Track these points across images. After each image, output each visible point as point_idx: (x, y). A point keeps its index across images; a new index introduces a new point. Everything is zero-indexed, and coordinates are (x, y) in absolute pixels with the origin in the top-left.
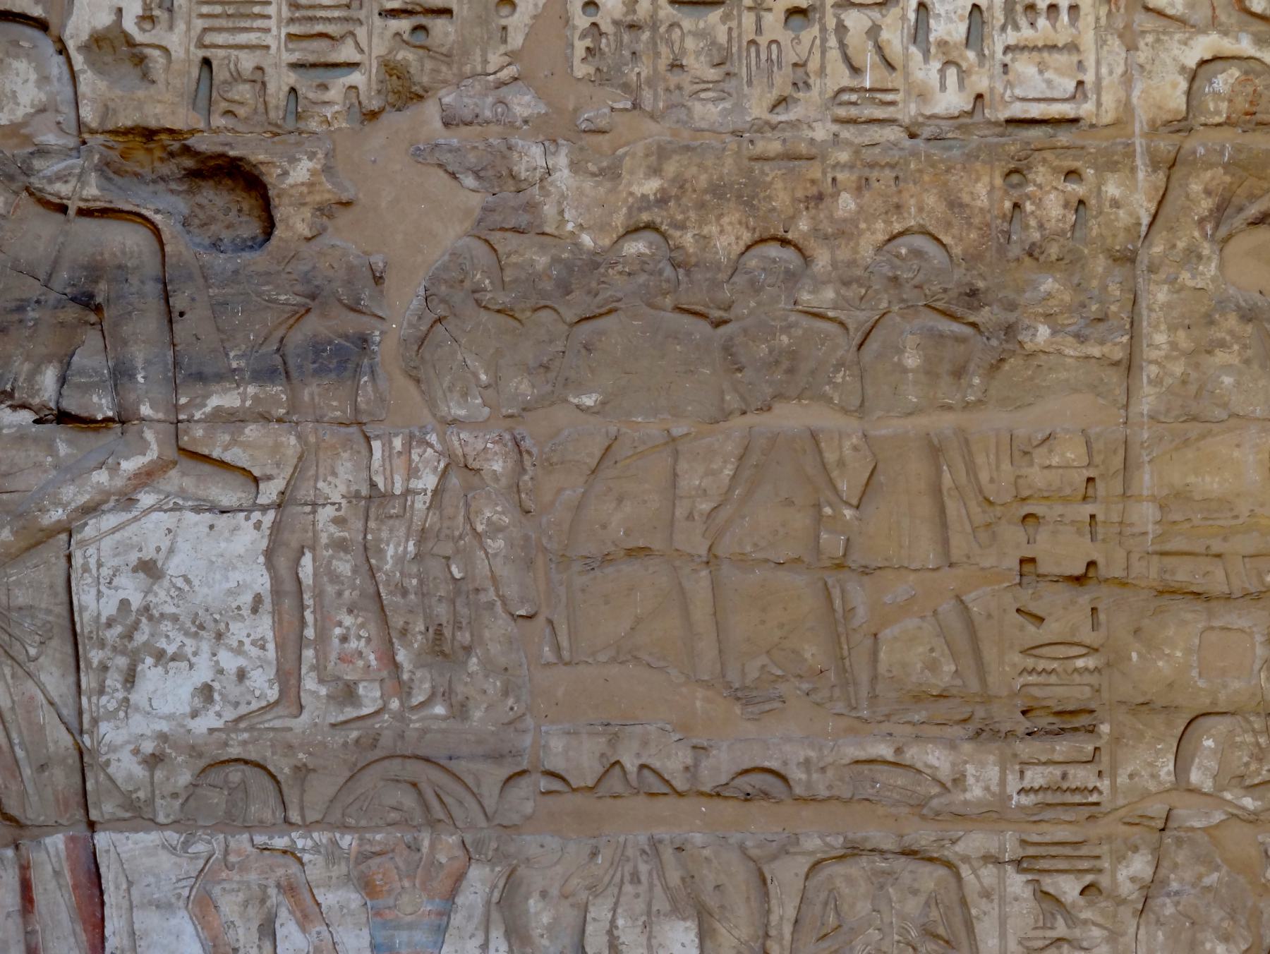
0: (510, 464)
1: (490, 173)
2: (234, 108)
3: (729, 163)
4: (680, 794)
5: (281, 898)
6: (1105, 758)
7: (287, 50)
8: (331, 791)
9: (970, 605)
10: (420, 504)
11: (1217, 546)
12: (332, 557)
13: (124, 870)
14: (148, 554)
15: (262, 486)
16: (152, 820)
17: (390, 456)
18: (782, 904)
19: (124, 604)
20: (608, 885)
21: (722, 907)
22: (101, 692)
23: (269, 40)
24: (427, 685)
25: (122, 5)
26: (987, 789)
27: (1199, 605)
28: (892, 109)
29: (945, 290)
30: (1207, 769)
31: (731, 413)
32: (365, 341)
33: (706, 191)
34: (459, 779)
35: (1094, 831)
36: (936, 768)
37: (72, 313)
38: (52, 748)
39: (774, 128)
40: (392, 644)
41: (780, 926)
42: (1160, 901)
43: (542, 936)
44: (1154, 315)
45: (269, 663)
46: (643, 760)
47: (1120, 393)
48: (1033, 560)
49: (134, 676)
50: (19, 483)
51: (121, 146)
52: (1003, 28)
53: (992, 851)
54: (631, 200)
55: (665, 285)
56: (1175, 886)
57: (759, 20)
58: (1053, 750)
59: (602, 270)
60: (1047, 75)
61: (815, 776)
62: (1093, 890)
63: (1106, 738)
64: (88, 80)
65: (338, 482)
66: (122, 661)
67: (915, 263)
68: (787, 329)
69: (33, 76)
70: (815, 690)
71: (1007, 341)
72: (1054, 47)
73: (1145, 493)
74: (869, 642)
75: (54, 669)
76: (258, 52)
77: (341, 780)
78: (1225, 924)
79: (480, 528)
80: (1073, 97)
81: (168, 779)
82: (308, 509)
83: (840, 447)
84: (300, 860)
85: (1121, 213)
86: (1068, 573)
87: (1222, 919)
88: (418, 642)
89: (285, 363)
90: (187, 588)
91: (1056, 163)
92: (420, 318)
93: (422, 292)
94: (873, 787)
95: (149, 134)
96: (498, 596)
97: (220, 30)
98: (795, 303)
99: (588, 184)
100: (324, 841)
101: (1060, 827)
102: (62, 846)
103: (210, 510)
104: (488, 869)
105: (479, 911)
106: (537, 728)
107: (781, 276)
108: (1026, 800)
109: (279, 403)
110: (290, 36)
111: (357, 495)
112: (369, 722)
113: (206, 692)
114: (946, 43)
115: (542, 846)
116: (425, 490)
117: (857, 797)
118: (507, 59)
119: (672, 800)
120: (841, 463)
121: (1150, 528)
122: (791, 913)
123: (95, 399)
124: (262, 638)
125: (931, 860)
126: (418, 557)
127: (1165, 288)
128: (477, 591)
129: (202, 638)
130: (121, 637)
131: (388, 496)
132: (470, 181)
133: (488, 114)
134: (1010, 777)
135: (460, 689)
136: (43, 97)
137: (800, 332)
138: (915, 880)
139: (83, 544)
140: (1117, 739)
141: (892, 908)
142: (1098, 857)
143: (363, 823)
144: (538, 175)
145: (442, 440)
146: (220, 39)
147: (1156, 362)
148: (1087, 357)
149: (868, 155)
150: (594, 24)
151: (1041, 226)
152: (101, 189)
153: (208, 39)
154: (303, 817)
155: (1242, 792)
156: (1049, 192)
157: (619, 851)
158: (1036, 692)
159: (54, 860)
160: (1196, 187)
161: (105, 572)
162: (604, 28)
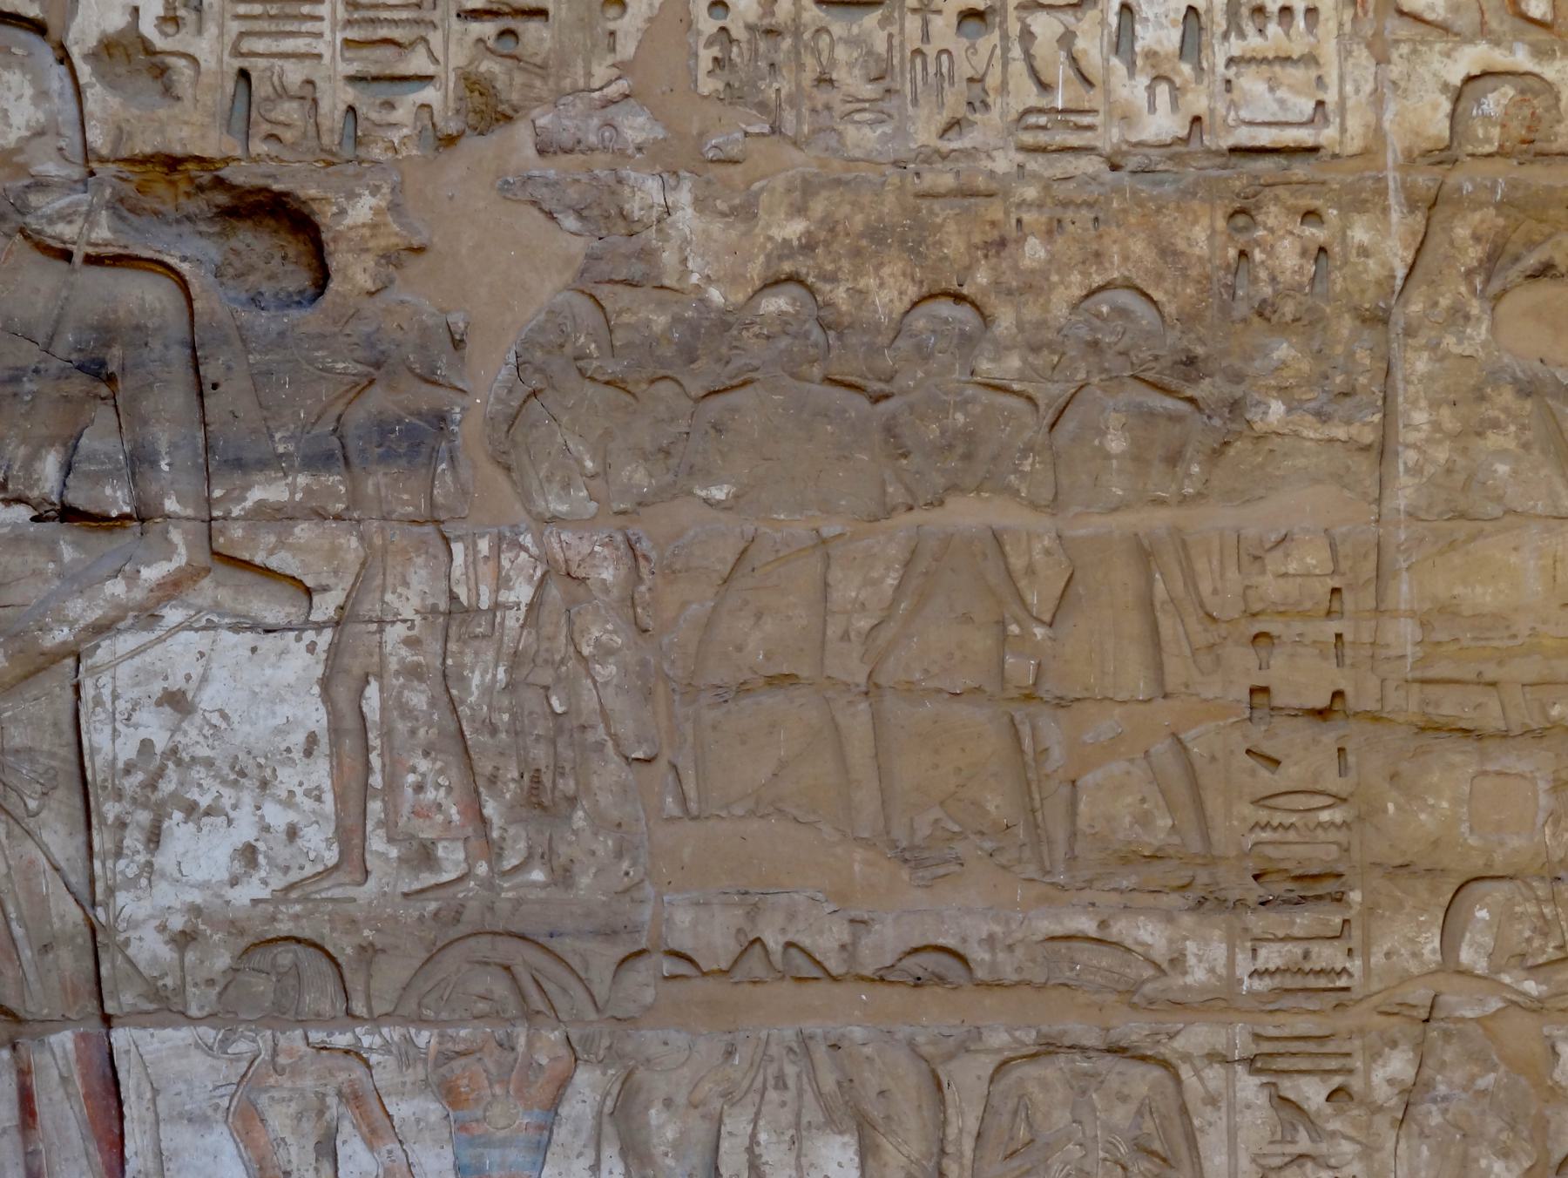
0: (623, 571)
1: (596, 212)
2: (278, 131)
4: (835, 979)
5: (342, 1109)
6: (1356, 932)
7: (344, 59)
8: (406, 975)
9: (1189, 745)
10: (512, 620)
11: (1491, 673)
12: (403, 687)
13: (148, 1075)
14: (176, 683)
15: (316, 599)
16: (183, 1013)
17: (475, 563)
18: (961, 1113)
19: (146, 745)
20: (746, 1093)
21: (888, 1118)
22: (119, 854)
23: (321, 47)
24: (522, 845)
26: (1212, 970)
27: (1470, 745)
28: (1089, 134)
29: (1156, 358)
30: (1481, 945)
31: (894, 509)
32: (443, 419)
33: (862, 235)
34: (560, 959)
35: (1343, 1022)
36: (1150, 946)
37: (78, 385)
38: (57, 925)
39: (944, 157)
41: (959, 1142)
42: (1424, 1107)
43: (666, 1154)
44: (1411, 389)
45: (327, 818)
46: (789, 937)
47: (1370, 484)
48: (1265, 690)
49: (159, 835)
50: (14, 596)
51: (136, 178)
52: (1226, 36)
53: (1219, 1047)
54: (769, 246)
55: (812, 351)
56: (1442, 1089)
57: (926, 23)
58: (1293, 923)
59: (734, 332)
60: (1280, 93)
62: (1341, 1094)
64: (96, 96)
65: (410, 594)
66: (144, 817)
67: (1119, 324)
68: (963, 404)
69: (28, 92)
70: (1000, 849)
71: (1232, 421)
72: (1288, 59)
73: (1403, 607)
74: (1065, 790)
75: (59, 826)
76: (308, 62)
77: (417, 964)
78: (1503, 1136)
79: (586, 651)
80: (1311, 121)
81: (202, 962)
82: (374, 627)
83: (1029, 550)
84: (366, 1062)
85: (1371, 263)
87: (1500, 1131)
89: (343, 447)
90: (224, 725)
91: (1291, 201)
92: (510, 391)
93: (512, 359)
94: (1072, 969)
95: (172, 163)
96: (609, 734)
98: (972, 373)
99: (717, 227)
100: (396, 1038)
101: (1300, 1018)
102: (70, 1046)
103: (252, 629)
104: (598, 1072)
105: (588, 1124)
106: (659, 895)
107: (955, 341)
108: (1259, 985)
109: (338, 499)
110: (347, 43)
111: (434, 610)
112: (451, 891)
113: (248, 854)
114: (1155, 54)
115: (666, 1043)
116: (518, 604)
117: (1053, 982)
118: (616, 72)
119: (825, 987)
120: (1031, 570)
121: (1409, 650)
122: (972, 1125)
123: (108, 491)
124: (318, 788)
125: (1144, 1058)
126: (510, 687)
127: (1425, 355)
128: (583, 728)
130: (143, 785)
131: (472, 611)
132: (570, 222)
133: (593, 139)
134: (1240, 957)
135: (563, 850)
136: (41, 117)
137: (978, 409)
138: (1124, 1083)
139: (95, 671)
140: (1370, 910)
141: (1097, 1118)
142: (1348, 1055)
143: (444, 1015)
144: (655, 214)
145: (539, 542)
146: (260, 45)
147: (1414, 446)
148: (1331, 440)
149: (1061, 191)
150: (723, 29)
151: (1273, 280)
152: (114, 231)
153: (246, 45)
155: (1523, 974)
156: (1283, 238)
158: (1270, 851)
159: (60, 1063)
160: (1462, 232)
161: (122, 705)
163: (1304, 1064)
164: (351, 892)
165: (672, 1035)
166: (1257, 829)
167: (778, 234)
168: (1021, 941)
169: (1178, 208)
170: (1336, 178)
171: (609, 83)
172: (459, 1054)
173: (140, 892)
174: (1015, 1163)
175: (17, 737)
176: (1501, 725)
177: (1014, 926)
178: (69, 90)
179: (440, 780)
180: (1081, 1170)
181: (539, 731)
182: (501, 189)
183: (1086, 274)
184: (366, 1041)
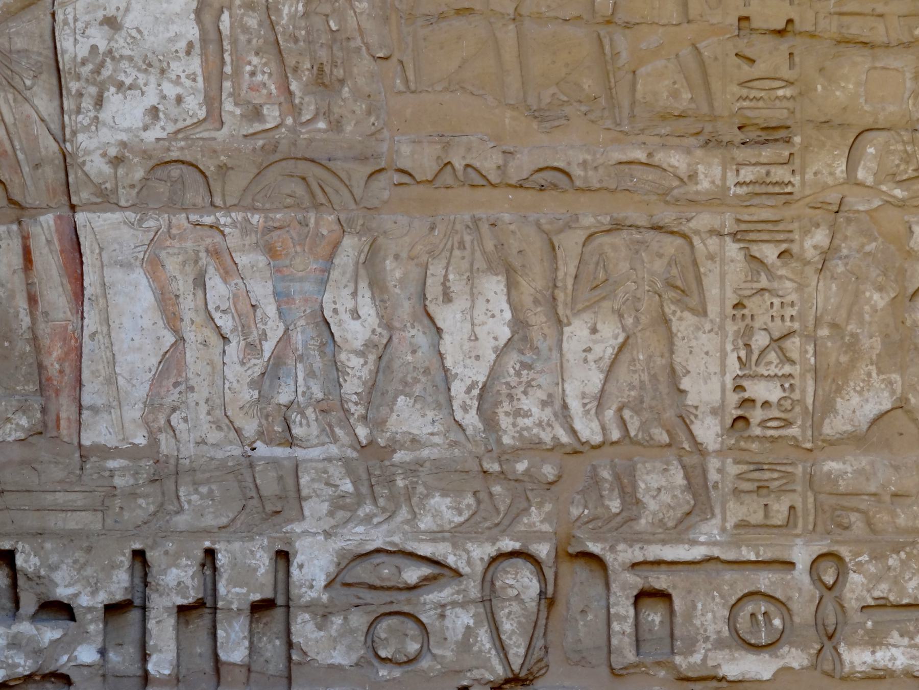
4: (494, 186)
5: (209, 259)
6: (797, 161)
8: (244, 183)
9: (702, 51)
12: (243, 15)
13: (97, 239)
14: (111, 12)
18: (566, 264)
19: (94, 48)
21: (523, 266)
22: (78, 111)
24: (312, 107)
26: (713, 182)
27: (866, 51)
34: (335, 174)
35: (788, 213)
36: (677, 168)
38: (44, 152)
40: (287, 77)
41: (564, 280)
42: (834, 262)
43: (395, 286)
46: (468, 161)
48: (747, 18)
53: (716, 226)
56: (845, 252)
58: (760, 155)
61: (590, 173)
62: (786, 254)
63: (798, 147)
66: (93, 90)
74: (630, 76)
75: (44, 96)
77: (252, 176)
78: (880, 279)
81: (127, 174)
84: (222, 232)
87: (878, 275)
88: (306, 76)
90: (139, 37)
94: (632, 181)
96: (363, 42)
100: (240, 219)
101: (764, 210)
102: (52, 223)
104: (356, 239)
105: (350, 269)
112: (271, 134)
113: (154, 112)
115: (395, 223)
119: (488, 189)
122: (572, 270)
124: (194, 74)
125: (672, 233)
126: (306, 15)
129: (150, 73)
130: (92, 72)
134: (729, 174)
135: (336, 110)
138: (661, 247)
140: (806, 147)
142: (791, 231)
143: (267, 206)
154: (225, 203)
155: (894, 185)
157: (450, 227)
158: (748, 113)
159: (46, 232)
161: (80, 25)
166: (741, 100)
168: (602, 164)
173: (91, 134)
174: (598, 292)
175: (19, 43)
176: (885, 40)
177: (598, 156)
179: (265, 69)
181: (323, 41)
184: (222, 220)
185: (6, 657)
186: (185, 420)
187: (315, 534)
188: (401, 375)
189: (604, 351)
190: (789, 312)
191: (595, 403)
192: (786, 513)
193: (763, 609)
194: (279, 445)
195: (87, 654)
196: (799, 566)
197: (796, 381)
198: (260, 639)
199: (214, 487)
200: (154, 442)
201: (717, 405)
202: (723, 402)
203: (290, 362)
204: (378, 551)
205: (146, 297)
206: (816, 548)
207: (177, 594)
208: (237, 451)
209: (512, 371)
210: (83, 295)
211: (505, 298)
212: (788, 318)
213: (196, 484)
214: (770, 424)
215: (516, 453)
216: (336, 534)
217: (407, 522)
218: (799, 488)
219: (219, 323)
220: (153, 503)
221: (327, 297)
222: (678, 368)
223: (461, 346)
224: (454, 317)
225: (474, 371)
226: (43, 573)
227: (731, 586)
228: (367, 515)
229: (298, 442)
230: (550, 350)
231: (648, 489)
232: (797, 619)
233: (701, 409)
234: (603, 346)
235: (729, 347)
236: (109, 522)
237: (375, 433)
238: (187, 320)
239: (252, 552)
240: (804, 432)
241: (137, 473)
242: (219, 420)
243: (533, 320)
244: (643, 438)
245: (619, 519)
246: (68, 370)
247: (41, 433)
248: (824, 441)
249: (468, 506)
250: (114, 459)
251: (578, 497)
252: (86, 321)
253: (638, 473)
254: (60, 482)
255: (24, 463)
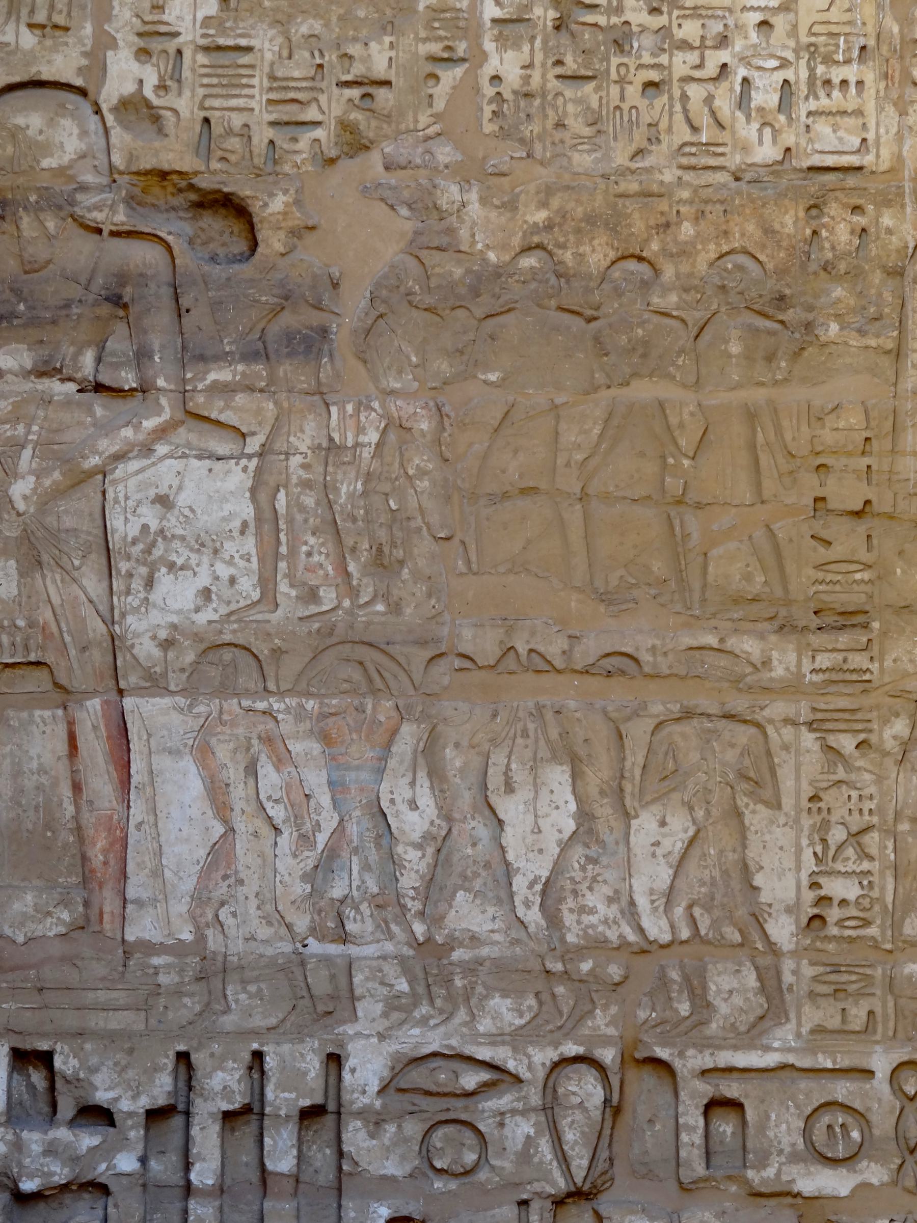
0: (434, 424)
1: (420, 205)
2: (227, 155)
3: (599, 198)
4: (559, 671)
5: (261, 747)
6: (876, 647)
7: (267, 111)
10: (366, 453)
12: (300, 493)
14: (163, 490)
15: (248, 440)
17: (344, 418)
18: (634, 754)
19: (145, 528)
22: (128, 592)
23: (253, 104)
24: (371, 589)
25: (142, 77)
26: (787, 669)
28: (722, 159)
29: (761, 296)
31: (599, 387)
33: (581, 220)
35: (867, 701)
37: (105, 309)
38: (91, 635)
39: (633, 172)
40: (345, 558)
41: (632, 771)
45: (254, 572)
46: (531, 646)
47: (890, 374)
48: (823, 499)
50: (67, 437)
51: (142, 184)
54: (525, 226)
55: (550, 291)
57: (622, 91)
58: (837, 641)
60: (839, 134)
61: (659, 659)
63: (876, 632)
64: (117, 134)
65: (304, 437)
66: (143, 570)
67: (738, 276)
68: (642, 324)
69: (76, 131)
70: (659, 594)
71: (807, 334)
72: (845, 112)
74: (700, 559)
75: (92, 576)
76: (245, 113)
77: (307, 660)
79: (411, 472)
80: (859, 151)
82: (282, 457)
83: (681, 414)
84: (275, 719)
85: (894, 238)
86: (850, 509)
88: (364, 557)
89: (265, 348)
90: (192, 516)
91: (845, 200)
92: (367, 314)
93: (368, 295)
95: (163, 175)
96: (424, 522)
97: (216, 96)
98: (648, 305)
99: (493, 215)
102: (98, 707)
103: (209, 458)
105: (409, 757)
106: (453, 621)
107: (638, 284)
108: (816, 678)
109: (261, 378)
110: (270, 101)
111: (319, 447)
112: (327, 616)
113: (206, 593)
114: (763, 109)
118: (433, 120)
119: (553, 676)
120: (681, 425)
122: (641, 760)
123: (123, 374)
124: (248, 554)
125: (745, 722)
126: (365, 494)
129: (203, 553)
130: (143, 552)
131: (342, 448)
132: (404, 211)
133: (418, 161)
134: (804, 661)
135: (395, 592)
137: (651, 327)
139: (114, 482)
140: (884, 633)
142: (869, 721)
143: (323, 691)
145: (383, 406)
146: (217, 103)
148: (867, 347)
149: (705, 193)
150: (498, 93)
151: (833, 248)
152: (128, 216)
153: (207, 103)
154: (278, 687)
156: (839, 223)
158: (824, 597)
161: (130, 503)
162: (505, 96)
163: (842, 726)
164: (267, 616)
165: (461, 705)
167: (531, 219)
169: (776, 204)
170: (873, 186)
171: (428, 127)
172: (331, 714)
174: (667, 783)
175: (68, 522)
177: (668, 641)
178: (101, 130)
180: (706, 788)
181: (382, 520)
182: (363, 191)
183: (718, 245)
184: (276, 706)
185: (42, 1165)
186: (234, 914)
187: (368, 1036)
188: (460, 869)
189: (674, 846)
190: (867, 805)
191: (664, 900)
192: (865, 1018)
193: (840, 1120)
194: (333, 941)
195: (127, 1163)
196: (879, 1075)
197: (875, 879)
198: (309, 1148)
199: (263, 986)
200: (201, 938)
201: (792, 903)
202: (798, 899)
203: (345, 854)
204: (435, 1055)
205: (195, 786)
206: (896, 1056)
207: (223, 1099)
208: (287, 947)
209: (576, 866)
210: (129, 783)
211: (569, 789)
212: (866, 812)
213: (244, 982)
214: (847, 923)
215: (580, 952)
216: (390, 1037)
217: (465, 1024)
218: (878, 993)
219: (271, 813)
220: (199, 1002)
221: (384, 787)
222: (751, 864)
223: (524, 839)
224: (517, 809)
225: (537, 865)
226: (82, 1075)
227: (807, 1095)
228: (423, 1016)
229: (353, 939)
230: (617, 843)
231: (719, 991)
232: (876, 1132)
233: (776, 907)
234: (672, 839)
235: (805, 842)
236: (153, 1022)
237: (432, 929)
238: (237, 809)
239: (302, 1055)
240: (883, 932)
241: (183, 970)
242: (269, 915)
243: (599, 812)
244: (714, 938)
245: (688, 1023)
246: (112, 862)
247: (83, 928)
248: (904, 942)
249: (530, 1008)
250: (158, 955)
251: (645, 999)
252: (132, 811)
253: (709, 974)
254: (103, 979)
255: (63, 959)
